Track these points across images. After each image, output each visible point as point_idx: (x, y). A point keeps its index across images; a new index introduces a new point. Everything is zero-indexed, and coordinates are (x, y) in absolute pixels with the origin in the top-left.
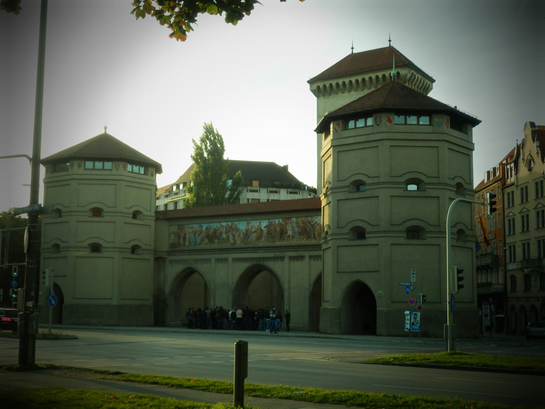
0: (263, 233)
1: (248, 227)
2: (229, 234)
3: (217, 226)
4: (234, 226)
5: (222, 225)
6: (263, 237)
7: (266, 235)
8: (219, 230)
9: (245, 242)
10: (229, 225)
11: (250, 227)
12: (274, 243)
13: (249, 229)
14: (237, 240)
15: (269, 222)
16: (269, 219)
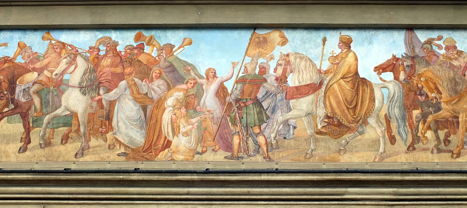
0: (372, 99)
1: (261, 60)
2: (112, 95)
3: (22, 47)
4: (155, 54)
5: (64, 44)
6: (372, 121)
7: (396, 111)
8: (40, 71)
9: (236, 140)
10: (119, 48)
11: (273, 64)
12: (459, 155)
13: (263, 70)
14: (175, 131)
15: (410, 44)
16: (410, 28)
